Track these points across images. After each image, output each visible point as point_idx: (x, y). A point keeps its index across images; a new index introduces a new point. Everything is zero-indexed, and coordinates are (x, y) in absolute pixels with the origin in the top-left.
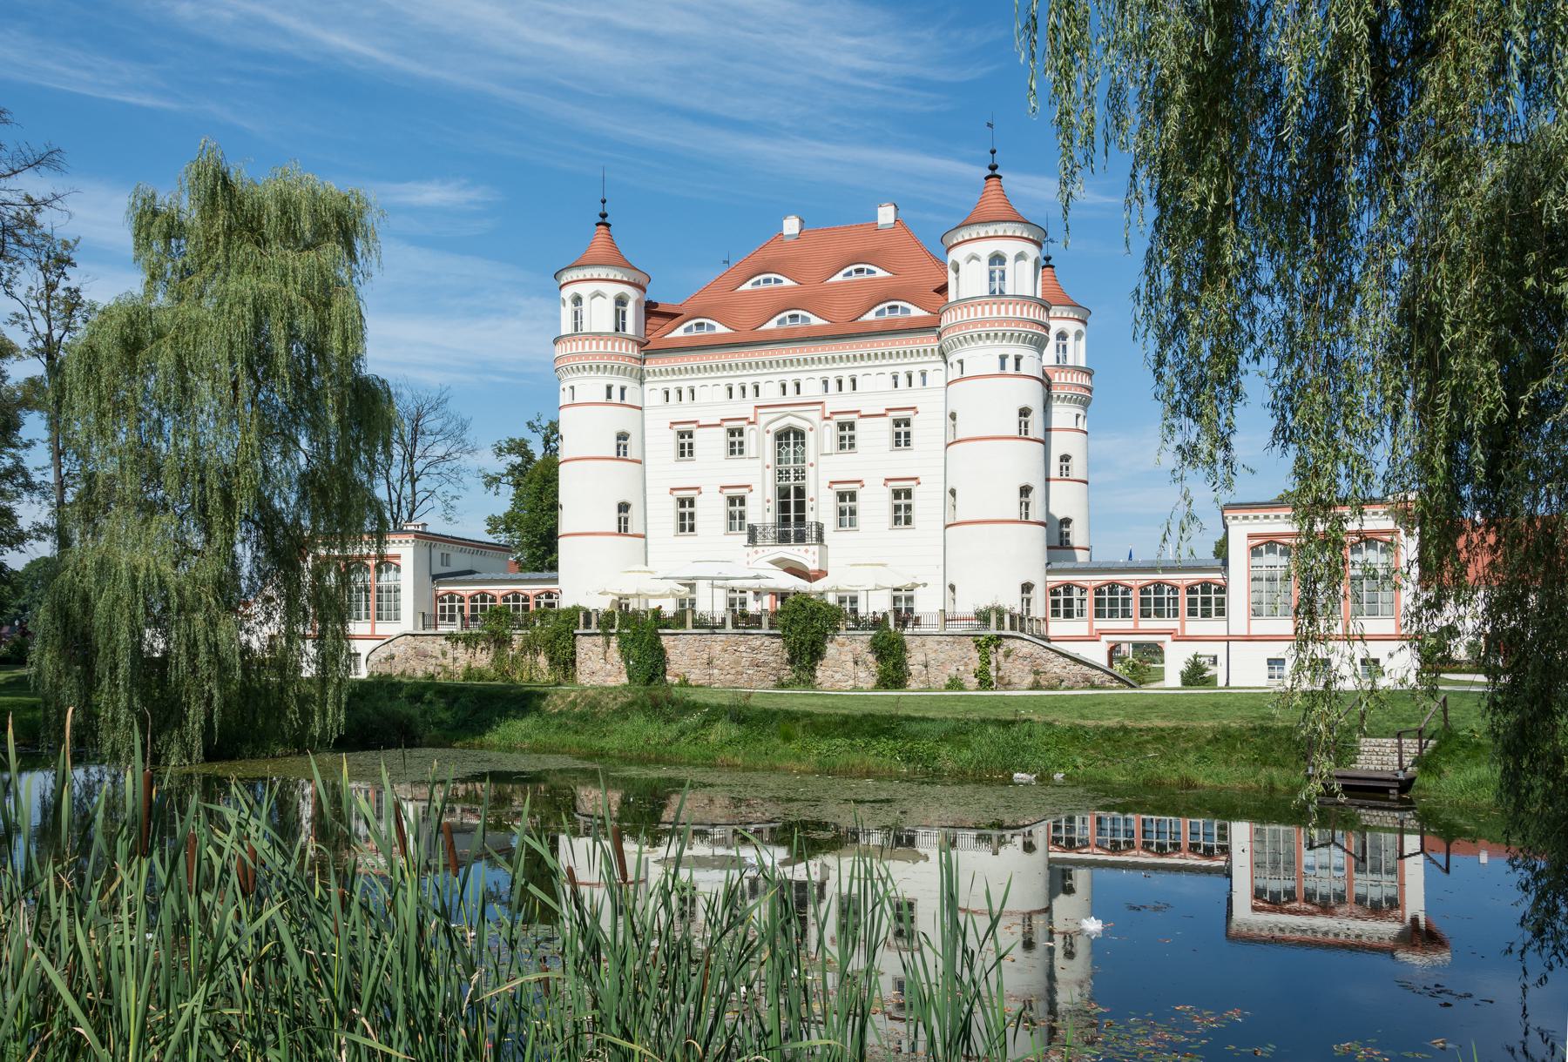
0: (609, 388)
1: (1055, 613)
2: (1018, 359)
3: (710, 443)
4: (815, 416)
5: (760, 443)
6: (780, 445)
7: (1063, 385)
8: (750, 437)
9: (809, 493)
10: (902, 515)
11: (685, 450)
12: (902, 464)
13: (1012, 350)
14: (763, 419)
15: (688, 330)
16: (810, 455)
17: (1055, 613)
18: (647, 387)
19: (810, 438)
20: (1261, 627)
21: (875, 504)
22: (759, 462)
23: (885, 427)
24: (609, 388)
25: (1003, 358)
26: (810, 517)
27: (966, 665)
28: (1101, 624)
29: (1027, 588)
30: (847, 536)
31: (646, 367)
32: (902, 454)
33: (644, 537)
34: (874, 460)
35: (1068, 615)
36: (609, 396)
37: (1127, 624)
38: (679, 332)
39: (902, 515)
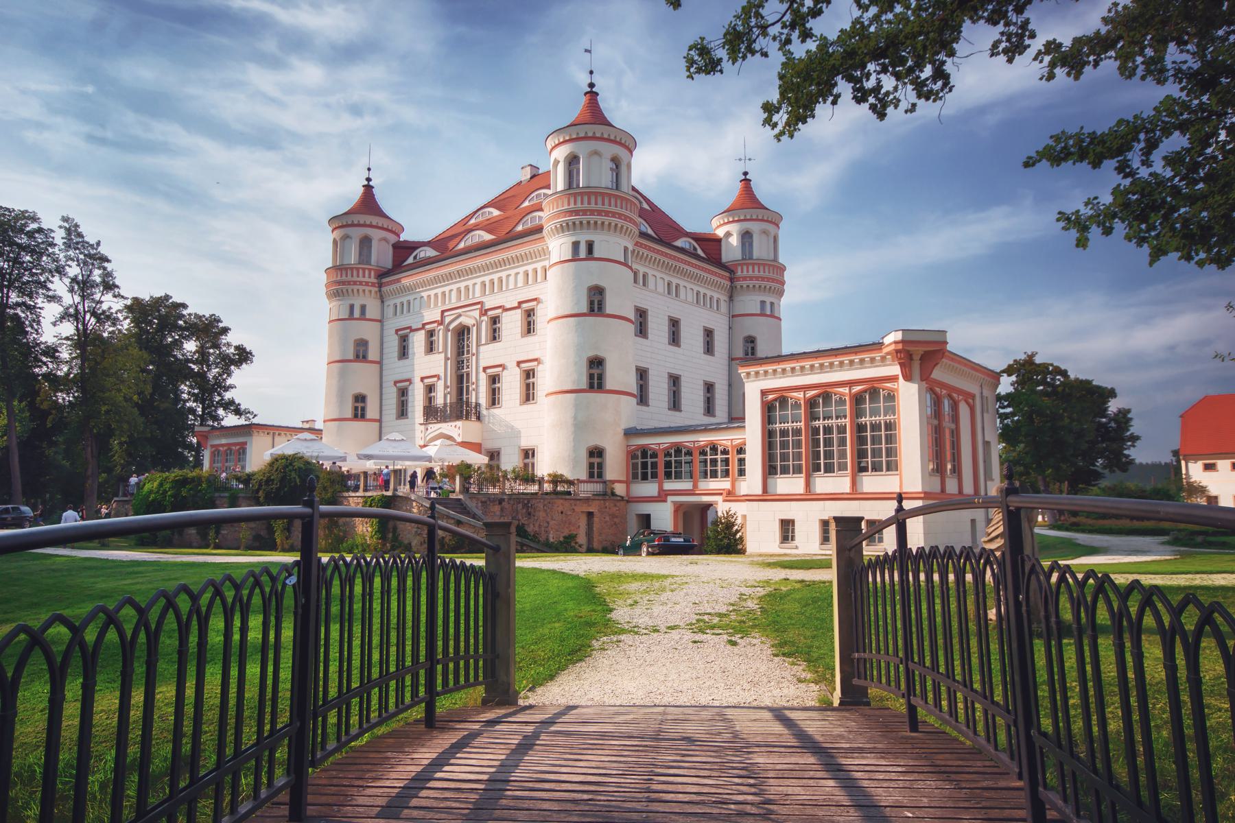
0: (352, 307)
1: (635, 476)
2: (590, 246)
3: (418, 341)
4: (476, 314)
5: (444, 340)
7: (745, 278)
8: (439, 339)
10: (528, 395)
11: (404, 352)
14: (447, 320)
17: (635, 476)
21: (511, 384)
23: (517, 315)
24: (352, 307)
28: (669, 485)
29: (596, 453)
30: (495, 411)
31: (384, 289)
32: (530, 339)
33: (380, 421)
35: (645, 478)
37: (685, 485)
38: (410, 260)
39: (528, 395)
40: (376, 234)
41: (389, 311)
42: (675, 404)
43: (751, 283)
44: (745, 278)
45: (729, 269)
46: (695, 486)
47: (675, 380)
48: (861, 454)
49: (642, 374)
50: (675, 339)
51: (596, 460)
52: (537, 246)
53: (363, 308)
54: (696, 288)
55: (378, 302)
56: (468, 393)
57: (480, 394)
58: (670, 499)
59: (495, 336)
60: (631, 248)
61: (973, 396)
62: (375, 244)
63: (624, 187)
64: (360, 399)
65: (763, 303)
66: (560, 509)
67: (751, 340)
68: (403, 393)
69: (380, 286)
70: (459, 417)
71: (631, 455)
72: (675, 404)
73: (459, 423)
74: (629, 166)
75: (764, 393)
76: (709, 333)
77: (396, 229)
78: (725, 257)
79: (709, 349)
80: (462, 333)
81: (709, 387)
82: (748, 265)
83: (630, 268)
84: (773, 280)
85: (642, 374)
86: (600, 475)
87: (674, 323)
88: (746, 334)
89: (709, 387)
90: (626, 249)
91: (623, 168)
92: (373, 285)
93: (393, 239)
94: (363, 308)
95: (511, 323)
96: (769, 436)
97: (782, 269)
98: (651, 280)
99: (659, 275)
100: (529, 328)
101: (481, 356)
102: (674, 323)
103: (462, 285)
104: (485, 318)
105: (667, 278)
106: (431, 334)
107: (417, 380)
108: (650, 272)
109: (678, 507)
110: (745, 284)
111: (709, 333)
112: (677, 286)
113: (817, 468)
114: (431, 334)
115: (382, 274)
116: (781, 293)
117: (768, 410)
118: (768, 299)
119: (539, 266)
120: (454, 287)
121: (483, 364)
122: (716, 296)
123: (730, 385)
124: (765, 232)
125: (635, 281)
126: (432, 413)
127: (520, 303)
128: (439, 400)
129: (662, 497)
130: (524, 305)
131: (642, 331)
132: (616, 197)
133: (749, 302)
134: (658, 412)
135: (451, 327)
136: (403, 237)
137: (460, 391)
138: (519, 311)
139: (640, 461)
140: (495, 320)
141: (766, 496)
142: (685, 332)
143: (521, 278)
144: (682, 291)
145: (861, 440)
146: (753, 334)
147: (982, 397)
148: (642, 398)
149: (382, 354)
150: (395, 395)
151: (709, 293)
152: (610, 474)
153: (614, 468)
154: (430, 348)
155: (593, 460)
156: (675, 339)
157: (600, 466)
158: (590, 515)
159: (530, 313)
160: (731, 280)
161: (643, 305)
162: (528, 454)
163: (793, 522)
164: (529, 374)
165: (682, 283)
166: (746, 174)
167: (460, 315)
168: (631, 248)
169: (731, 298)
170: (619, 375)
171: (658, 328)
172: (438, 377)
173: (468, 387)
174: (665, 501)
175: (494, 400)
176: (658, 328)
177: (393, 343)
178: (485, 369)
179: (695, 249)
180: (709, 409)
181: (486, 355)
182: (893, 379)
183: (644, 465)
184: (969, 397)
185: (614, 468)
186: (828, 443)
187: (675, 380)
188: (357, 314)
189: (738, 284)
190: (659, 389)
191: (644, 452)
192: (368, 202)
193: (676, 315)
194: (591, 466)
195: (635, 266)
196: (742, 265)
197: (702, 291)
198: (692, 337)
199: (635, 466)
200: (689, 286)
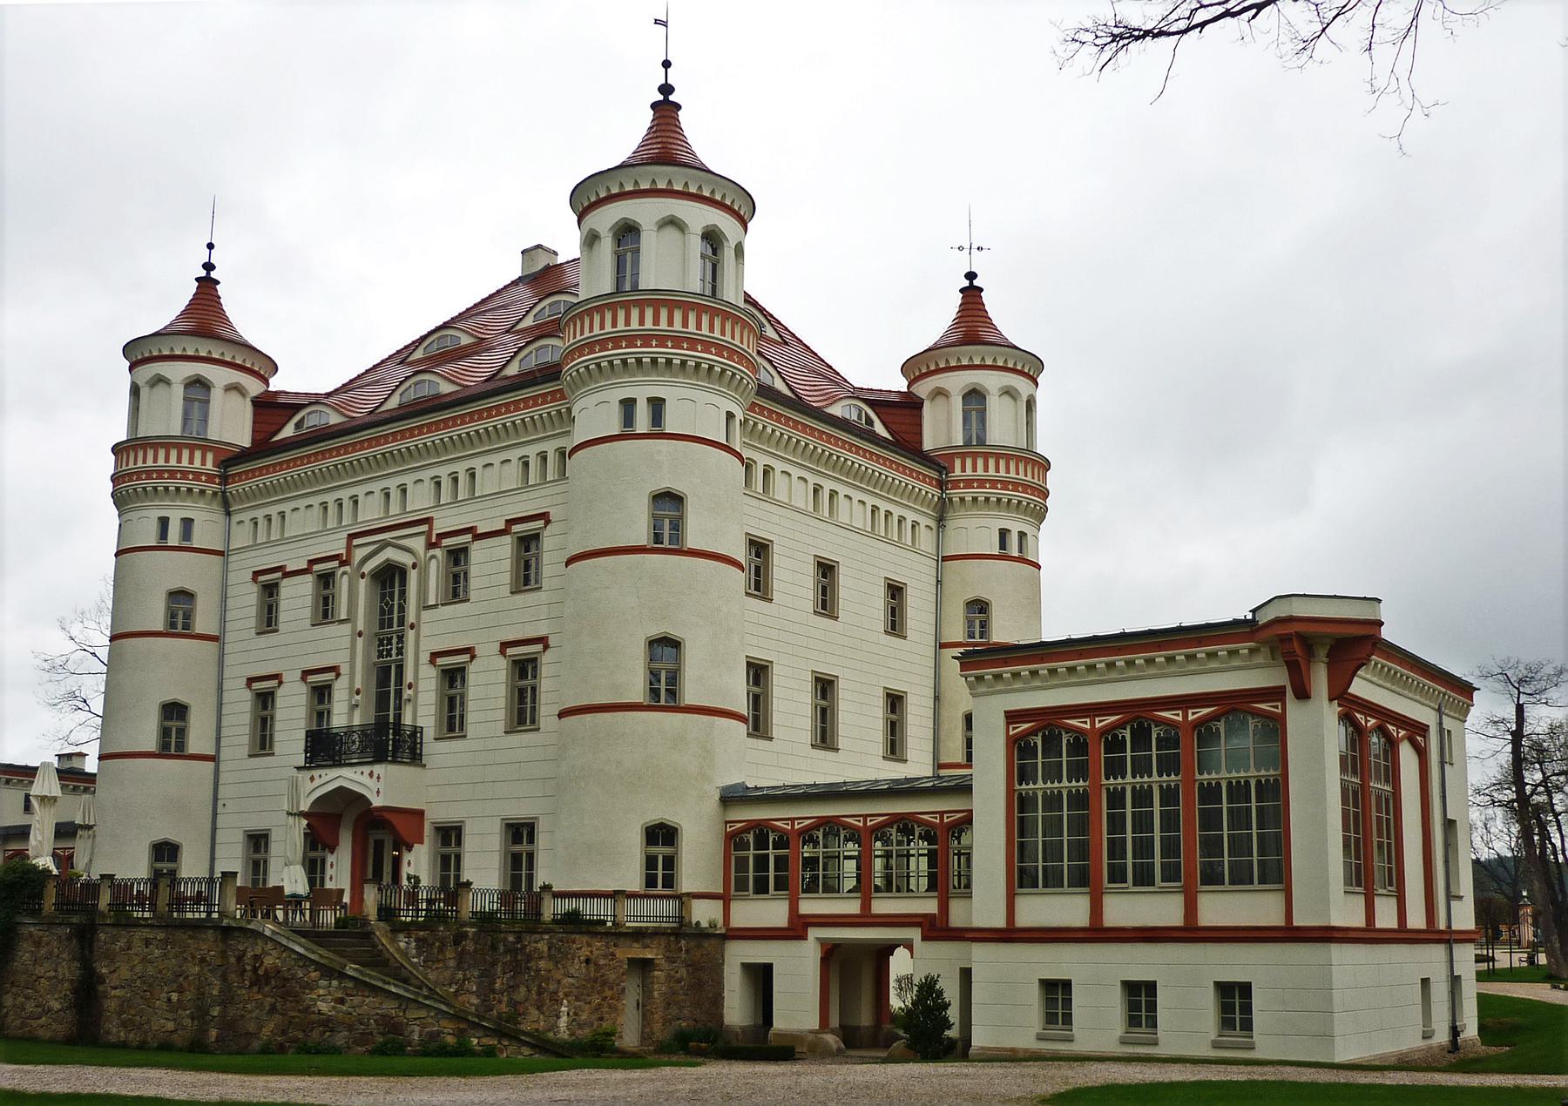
0: (164, 522)
4: (418, 544)
5: (355, 595)
6: (383, 597)
7: (969, 483)
9: (409, 677)
12: (526, 616)
13: (642, 392)
14: (359, 554)
15: (298, 425)
16: (411, 617)
17: (741, 885)
18: (235, 518)
19: (413, 576)
20: (1037, 910)
22: (347, 628)
23: (504, 548)
25: (628, 405)
26: (407, 720)
27: (180, 990)
29: (662, 834)
31: (232, 488)
34: (488, 616)
35: (761, 888)
36: (164, 533)
38: (288, 431)
40: (219, 376)
41: (241, 537)
42: (825, 737)
43: (981, 493)
44: (969, 483)
45: (938, 464)
46: (866, 905)
47: (825, 686)
48: (1212, 846)
49: (758, 672)
50: (826, 603)
51: (661, 851)
52: (551, 408)
53: (187, 523)
54: (870, 501)
55: (219, 517)
56: (399, 708)
57: (422, 710)
58: (813, 933)
59: (456, 589)
60: (739, 415)
61: (1423, 729)
62: (217, 395)
63: (730, 294)
64: (174, 712)
65: (1004, 534)
66: (585, 952)
67: (979, 607)
68: (265, 700)
69: (225, 480)
70: (380, 758)
71: (734, 840)
72: (825, 737)
73: (378, 769)
74: (739, 251)
75: (1012, 717)
76: (895, 591)
77: (264, 366)
78: (930, 441)
79: (895, 624)
80: (389, 578)
81: (895, 701)
82: (975, 456)
83: (739, 456)
84: (1026, 487)
85: (758, 672)
86: (669, 881)
87: (826, 569)
88: (971, 596)
89: (895, 701)
90: (730, 416)
91: (728, 253)
92: (210, 478)
93: (254, 387)
94: (187, 523)
95: (491, 563)
96: (1020, 806)
97: (1045, 465)
98: (779, 483)
99: (796, 472)
100: (525, 576)
101: (425, 630)
102: (826, 569)
103: (392, 484)
104: (437, 552)
105: (813, 479)
106: (326, 580)
107: (292, 677)
108: (779, 466)
109: (831, 952)
110: (968, 494)
111: (895, 591)
112: (833, 494)
113: (1117, 875)
114: (326, 580)
115: (231, 460)
116: (1040, 514)
117: (1019, 748)
118: (1015, 527)
119: (550, 447)
120: (376, 487)
121: (429, 645)
122: (910, 517)
123: (937, 698)
124: (1009, 392)
125: (748, 483)
126: (323, 747)
127: (510, 522)
128: (339, 718)
129: (797, 929)
130: (516, 528)
131: (760, 585)
132: (713, 313)
133: (976, 531)
134: (788, 760)
135: (367, 569)
136: (276, 384)
137: (382, 701)
138: (507, 539)
139: (751, 852)
140: (458, 556)
141: (1010, 934)
142: (847, 585)
143: (514, 469)
144: (841, 500)
145: (1210, 820)
146: (984, 596)
147: (1441, 730)
148: (758, 722)
149: (223, 621)
150: (248, 706)
151: (897, 512)
152: (688, 881)
153: (699, 864)
154: (325, 612)
155: (654, 850)
156: (826, 603)
157: (670, 862)
158: (644, 966)
159: (528, 543)
160: (941, 485)
161: (762, 533)
162: (520, 832)
163: (1067, 985)
164: (524, 669)
165: (842, 490)
166: (971, 276)
167: (385, 545)
168: (739, 415)
169: (941, 520)
170: (713, 676)
171: (793, 578)
172: (334, 669)
173: (399, 693)
174: (804, 937)
175: (453, 722)
176: (793, 578)
177: (247, 599)
178: (435, 655)
179: (870, 422)
180: (894, 748)
181: (434, 629)
182: (1276, 694)
183: (762, 863)
184: (1417, 730)
185: (699, 864)
186: (1143, 823)
187: (825, 686)
188: (174, 538)
189: (956, 494)
190: (792, 705)
191: (761, 831)
192: (205, 308)
193: (828, 554)
194: (651, 862)
195: (746, 454)
196: (963, 456)
197: (884, 506)
198: (861, 596)
199: (742, 864)
200: (857, 496)
